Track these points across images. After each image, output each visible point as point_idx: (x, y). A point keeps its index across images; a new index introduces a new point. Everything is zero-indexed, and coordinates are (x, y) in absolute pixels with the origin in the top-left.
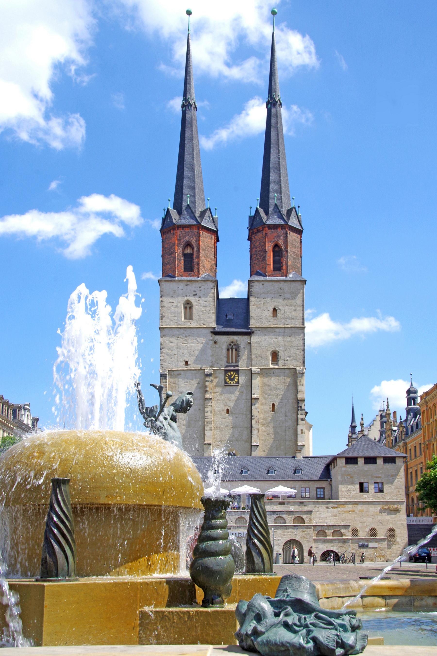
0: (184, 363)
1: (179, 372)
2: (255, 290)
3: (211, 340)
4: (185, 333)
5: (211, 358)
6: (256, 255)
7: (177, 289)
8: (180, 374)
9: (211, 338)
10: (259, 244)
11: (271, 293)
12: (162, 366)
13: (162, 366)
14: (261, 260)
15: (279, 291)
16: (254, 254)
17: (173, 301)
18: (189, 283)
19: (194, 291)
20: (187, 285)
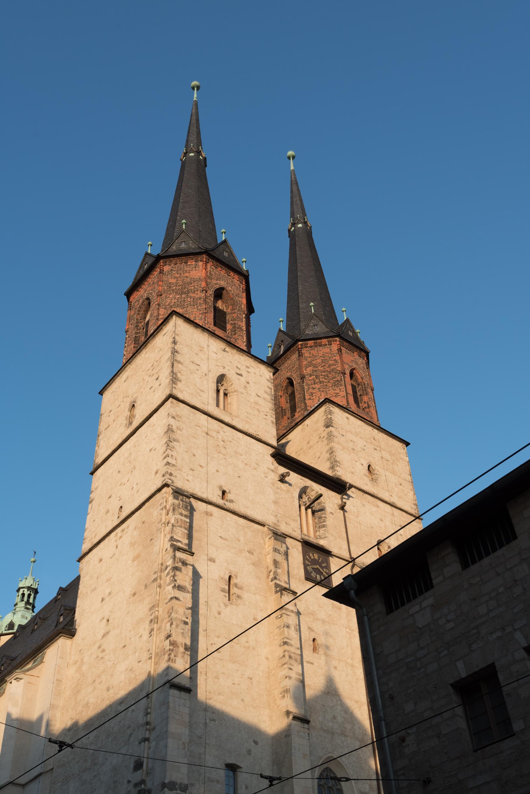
0: (220, 493)
1: (210, 508)
2: (336, 419)
3: (272, 471)
4: (222, 433)
5: (273, 507)
6: (317, 377)
7: (206, 347)
8: (211, 515)
9: (272, 467)
10: (322, 362)
11: (361, 438)
12: (172, 478)
13: (172, 478)
14: (330, 385)
15: (373, 440)
16: (311, 375)
17: (198, 363)
18: (228, 349)
19: (237, 367)
20: (224, 350)
